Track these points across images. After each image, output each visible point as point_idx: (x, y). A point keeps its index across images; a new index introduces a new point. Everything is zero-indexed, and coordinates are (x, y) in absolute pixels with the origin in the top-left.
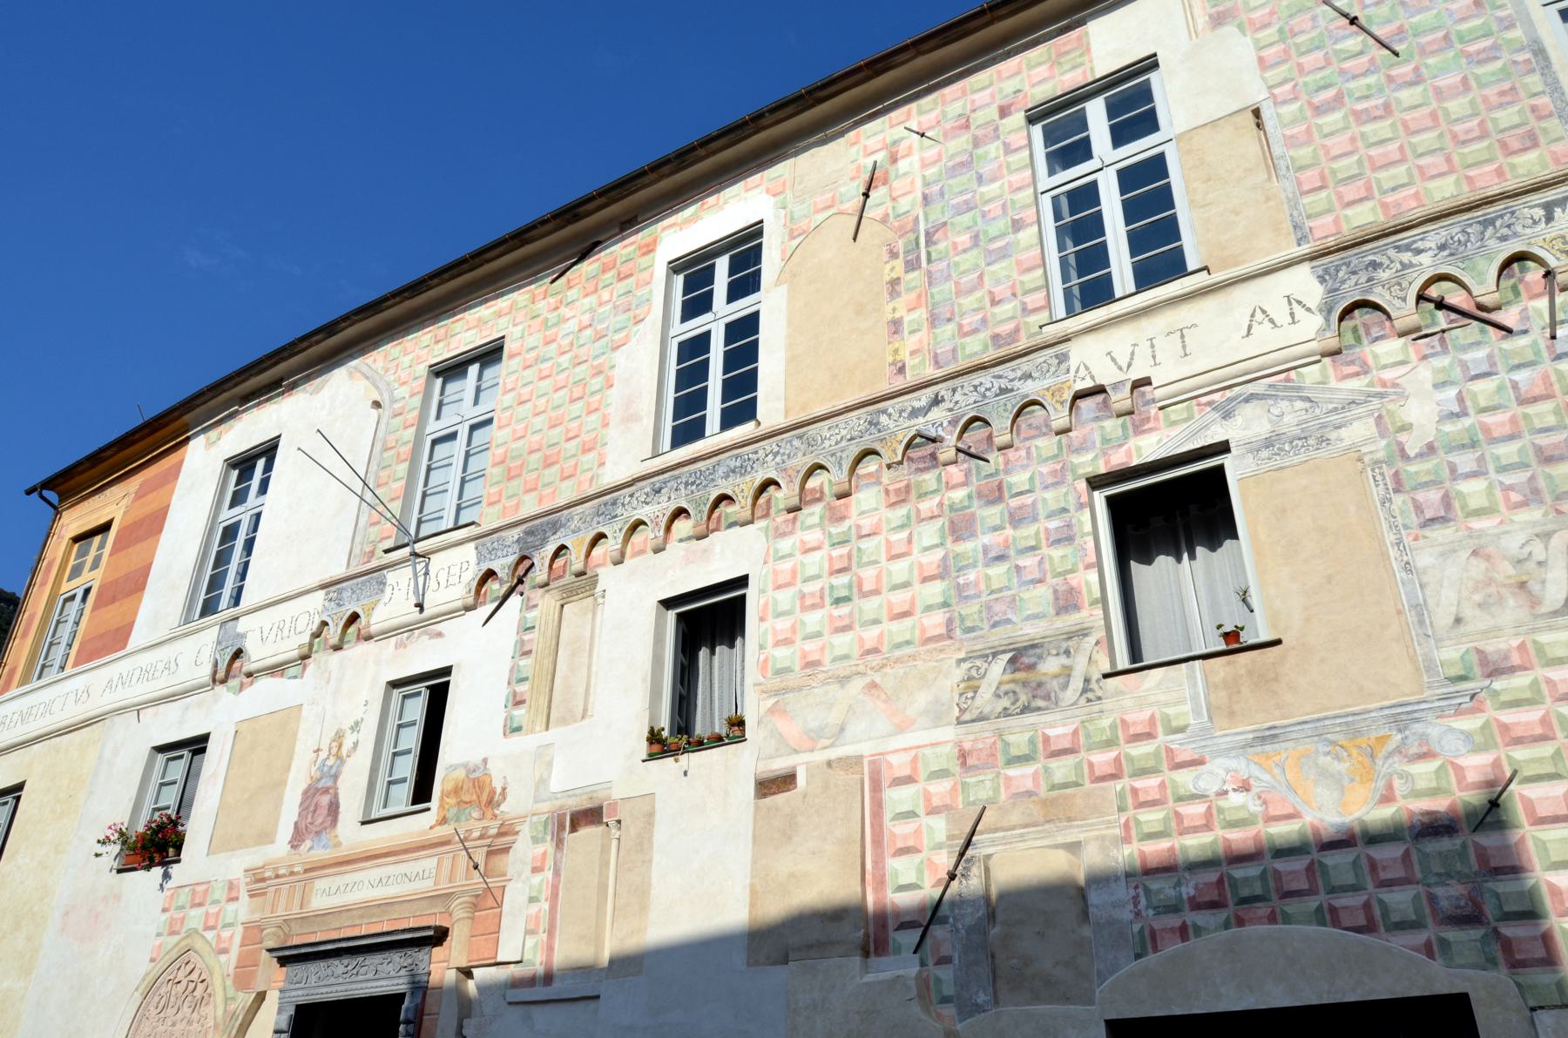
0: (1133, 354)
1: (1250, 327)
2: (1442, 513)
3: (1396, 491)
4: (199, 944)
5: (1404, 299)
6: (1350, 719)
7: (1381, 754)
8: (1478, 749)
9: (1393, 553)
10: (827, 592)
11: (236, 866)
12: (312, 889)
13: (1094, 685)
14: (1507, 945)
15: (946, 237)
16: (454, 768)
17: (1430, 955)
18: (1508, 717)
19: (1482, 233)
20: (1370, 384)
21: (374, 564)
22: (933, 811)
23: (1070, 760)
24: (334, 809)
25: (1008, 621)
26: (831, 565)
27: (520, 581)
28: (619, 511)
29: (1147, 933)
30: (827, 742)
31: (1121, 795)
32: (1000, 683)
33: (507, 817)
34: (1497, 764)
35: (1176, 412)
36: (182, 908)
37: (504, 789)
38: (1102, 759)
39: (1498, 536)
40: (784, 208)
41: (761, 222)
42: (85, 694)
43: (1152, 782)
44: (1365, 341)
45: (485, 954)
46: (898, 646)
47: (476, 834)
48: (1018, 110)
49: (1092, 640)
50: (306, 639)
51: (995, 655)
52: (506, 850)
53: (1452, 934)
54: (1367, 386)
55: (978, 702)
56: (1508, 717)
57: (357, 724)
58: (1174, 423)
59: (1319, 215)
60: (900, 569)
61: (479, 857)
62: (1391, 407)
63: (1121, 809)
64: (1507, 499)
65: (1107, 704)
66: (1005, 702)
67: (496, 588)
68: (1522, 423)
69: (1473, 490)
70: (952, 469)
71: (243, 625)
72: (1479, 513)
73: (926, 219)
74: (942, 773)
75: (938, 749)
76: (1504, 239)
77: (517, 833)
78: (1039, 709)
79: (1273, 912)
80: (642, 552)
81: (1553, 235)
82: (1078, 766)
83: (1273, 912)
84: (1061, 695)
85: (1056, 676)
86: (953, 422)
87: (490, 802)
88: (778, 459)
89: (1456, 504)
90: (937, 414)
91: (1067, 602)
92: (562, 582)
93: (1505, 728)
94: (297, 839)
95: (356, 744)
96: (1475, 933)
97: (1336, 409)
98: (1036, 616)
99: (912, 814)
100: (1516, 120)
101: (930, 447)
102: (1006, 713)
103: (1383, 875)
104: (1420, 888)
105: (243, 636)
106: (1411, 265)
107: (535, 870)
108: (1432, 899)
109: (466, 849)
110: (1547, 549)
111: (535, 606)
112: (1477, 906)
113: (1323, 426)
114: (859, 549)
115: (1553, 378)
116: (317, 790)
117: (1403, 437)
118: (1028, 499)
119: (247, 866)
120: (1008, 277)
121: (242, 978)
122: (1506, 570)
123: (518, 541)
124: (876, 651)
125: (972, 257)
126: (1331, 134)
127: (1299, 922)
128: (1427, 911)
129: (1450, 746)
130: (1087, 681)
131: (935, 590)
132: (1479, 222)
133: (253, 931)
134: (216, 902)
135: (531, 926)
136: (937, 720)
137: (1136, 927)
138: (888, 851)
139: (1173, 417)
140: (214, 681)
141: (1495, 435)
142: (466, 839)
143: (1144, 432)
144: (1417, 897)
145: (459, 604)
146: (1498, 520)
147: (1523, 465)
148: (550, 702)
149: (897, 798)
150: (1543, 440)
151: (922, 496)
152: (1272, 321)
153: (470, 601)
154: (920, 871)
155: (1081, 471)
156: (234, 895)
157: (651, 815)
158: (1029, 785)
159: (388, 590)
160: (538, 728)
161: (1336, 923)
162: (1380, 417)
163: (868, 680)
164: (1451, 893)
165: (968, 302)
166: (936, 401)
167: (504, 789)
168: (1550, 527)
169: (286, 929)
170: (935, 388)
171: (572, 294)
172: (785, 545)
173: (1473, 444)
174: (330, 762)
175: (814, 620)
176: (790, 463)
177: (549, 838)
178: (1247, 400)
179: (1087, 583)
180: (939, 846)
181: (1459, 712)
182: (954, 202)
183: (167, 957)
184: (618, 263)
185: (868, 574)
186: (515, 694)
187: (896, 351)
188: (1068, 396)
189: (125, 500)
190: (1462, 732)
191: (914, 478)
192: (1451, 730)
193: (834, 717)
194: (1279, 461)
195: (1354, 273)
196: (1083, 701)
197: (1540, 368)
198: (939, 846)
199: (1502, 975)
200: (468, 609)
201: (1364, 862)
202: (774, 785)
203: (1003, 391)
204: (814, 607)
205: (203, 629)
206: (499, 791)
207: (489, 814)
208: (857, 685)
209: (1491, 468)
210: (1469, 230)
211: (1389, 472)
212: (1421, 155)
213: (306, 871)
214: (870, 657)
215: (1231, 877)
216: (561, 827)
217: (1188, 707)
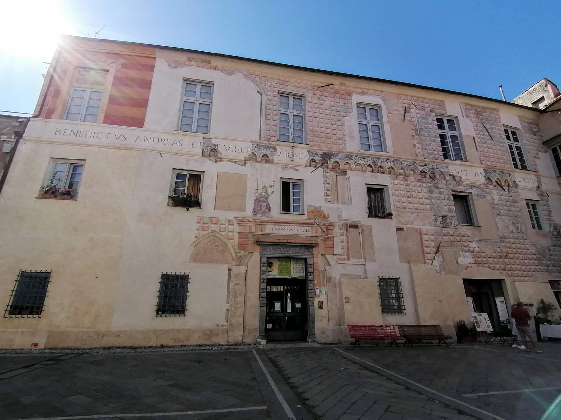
8: (504, 248)
22: (431, 241)
25: (441, 211)
32: (441, 222)
37: (328, 215)
38: (458, 238)
43: (466, 243)
46: (422, 209)
49: (455, 218)
51: (439, 216)
52: (333, 229)
60: (420, 195)
61: (325, 229)
63: (461, 247)
87: (324, 217)
90: (425, 167)
91: (450, 211)
92: (335, 170)
93: (507, 246)
94: (255, 212)
95: (273, 192)
96: (505, 272)
99: (428, 241)
101: (424, 174)
102: (442, 227)
105: (215, 145)
107: (341, 235)
112: (505, 268)
113: (484, 195)
117: (494, 201)
123: (321, 155)
124: (417, 209)
125: (428, 139)
131: (427, 201)
135: (342, 248)
136: (431, 224)
137: (465, 265)
149: (425, 237)
151: (423, 182)
153: (309, 165)
157: (371, 230)
158: (447, 240)
167: (328, 215)
169: (257, 237)
170: (426, 162)
172: (396, 182)
174: (264, 194)
175: (404, 199)
177: (344, 229)
180: (433, 247)
183: (203, 237)
185: (414, 194)
187: (415, 151)
193: (411, 219)
198: (433, 247)
199: (508, 277)
203: (437, 168)
206: (327, 215)
208: (414, 215)
213: (261, 222)
216: (347, 227)
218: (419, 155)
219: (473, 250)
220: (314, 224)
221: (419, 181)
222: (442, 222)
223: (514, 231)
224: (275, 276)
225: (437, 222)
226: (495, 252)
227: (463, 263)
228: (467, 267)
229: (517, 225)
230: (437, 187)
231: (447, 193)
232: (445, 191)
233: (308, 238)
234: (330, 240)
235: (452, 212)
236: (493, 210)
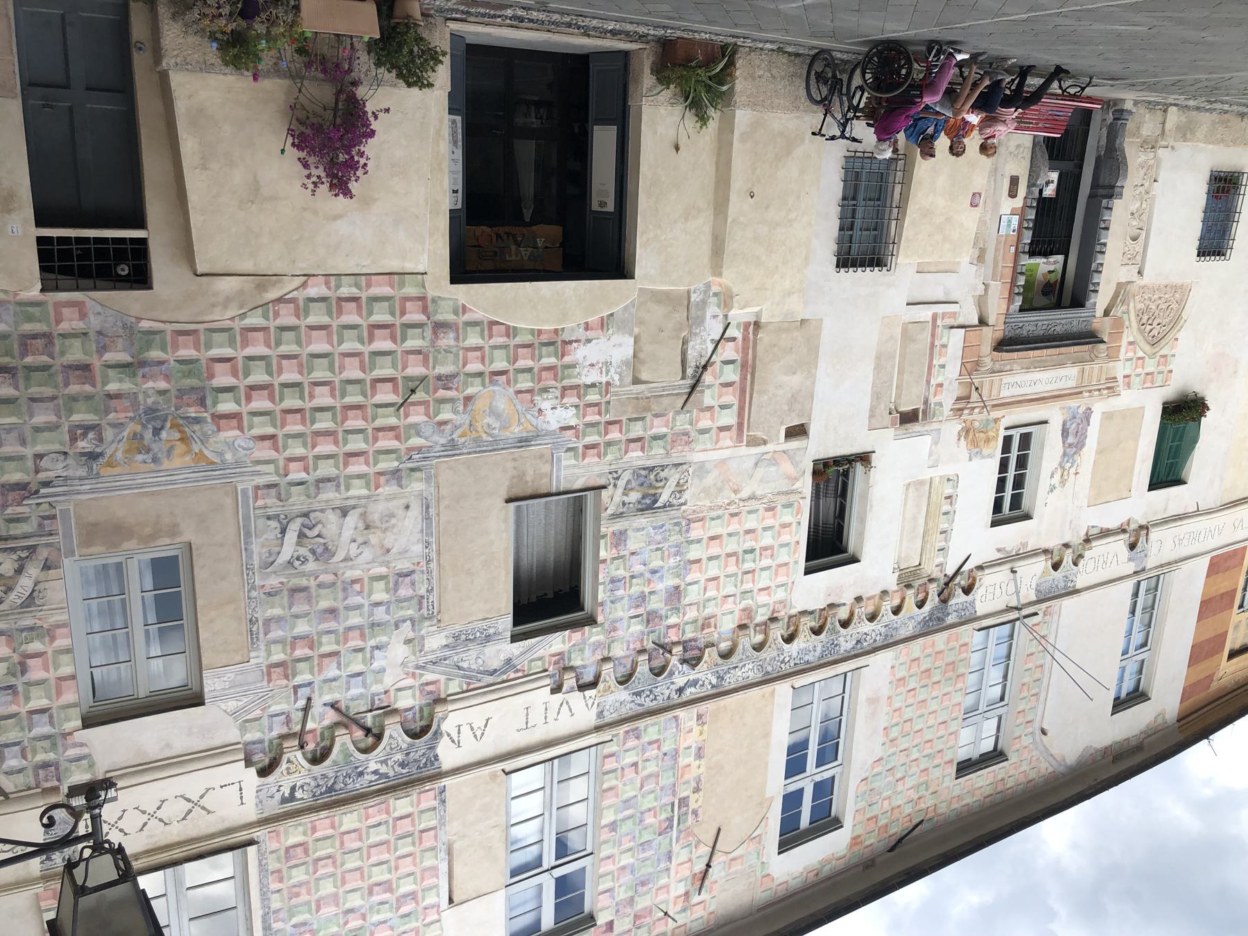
0: (558, 713)
1: (486, 726)
2: (401, 579)
3: (422, 597)
4: (1147, 348)
5: (391, 737)
6: (478, 449)
7: (466, 426)
8: (414, 426)
9: (434, 555)
10: (758, 558)
11: (1126, 399)
12: (1077, 380)
13: (612, 481)
14: (425, 310)
15: (660, 823)
16: (990, 456)
17: (464, 307)
18: (394, 444)
19: (335, 782)
20: (422, 675)
21: (1044, 605)
22: (710, 408)
23: (632, 435)
24: (1065, 433)
26: (754, 576)
27: (947, 584)
28: (883, 630)
29: (605, 328)
30: (765, 456)
31: (607, 411)
32: (663, 487)
33: (957, 421)
34: (407, 415)
35: (538, 666)
36: (1159, 373)
38: (614, 435)
39: (373, 561)
40: (763, 863)
41: (779, 853)
42: (1236, 525)
43: (589, 419)
44: (417, 708)
45: (972, 334)
46: (719, 517)
47: (977, 410)
48: (601, 926)
49: (609, 512)
50: (1087, 554)
51: (665, 506)
52: (958, 399)
53: (450, 317)
54: (423, 675)
55: (677, 476)
56: (394, 444)
57: (1052, 491)
58: (540, 659)
59: (429, 810)
60: (713, 569)
61: (975, 396)
62: (413, 658)
63: (608, 403)
64: (362, 587)
65: (607, 469)
66: (662, 475)
67: (961, 580)
69: (380, 595)
70: (675, 639)
71: (1131, 568)
72: (380, 578)
73: (671, 840)
74: (703, 432)
75: (704, 447)
76: (324, 776)
77: (952, 410)
78: (644, 469)
79: (539, 336)
80: (869, 599)
81: (294, 776)
82: (628, 431)
83: (539, 336)
84: (631, 477)
85: (632, 489)
86: (671, 674)
87: (968, 432)
88: (782, 657)
89: (391, 585)
90: (680, 681)
91: (620, 538)
93: (398, 438)
95: (1052, 476)
96: (440, 317)
97: (445, 660)
98: (638, 530)
99: (722, 407)
100: (294, 872)
101: (688, 655)
102: (663, 468)
103: (478, 354)
104: (461, 345)
105: (1130, 560)
106: (382, 762)
107: (941, 385)
108: (457, 339)
109: (983, 401)
111: (937, 566)
112: (435, 333)
113: (454, 648)
114: (736, 587)
115: (316, 669)
116: (1076, 447)
117: (411, 635)
118: (633, 612)
119: (1118, 397)
120: (625, 785)
121: (1119, 325)
122: (374, 539)
123: (948, 614)
124: (733, 515)
126: (409, 875)
127: (526, 329)
128: (461, 331)
129: (428, 431)
130: (615, 485)
131: (694, 553)
132: (335, 791)
133: (1113, 356)
134: (1138, 375)
135: (944, 350)
136: (702, 468)
137: (610, 331)
138: (737, 385)
139: (539, 663)
140: (1147, 528)
142: (983, 408)
143: (558, 654)
144: (464, 340)
145: (987, 571)
147: (347, 608)
148: (929, 497)
149: (729, 418)
150: (332, 625)
152: (472, 729)
154: (721, 371)
155: (599, 629)
156: (1127, 379)
158: (657, 421)
159: (1034, 586)
160: (937, 479)
161: (508, 327)
162: (421, 651)
163: (739, 496)
164: (447, 340)
165: (652, 768)
166: (680, 691)
168: (342, 565)
169: (1092, 355)
170: (680, 701)
171: (908, 810)
172: (780, 594)
173: (373, 625)
174: (1069, 465)
175: (767, 539)
176: (775, 653)
178: (495, 671)
179: (606, 550)
180: (709, 387)
181: (419, 449)
182: (652, 852)
184: (876, 832)
185: (732, 569)
186: (951, 504)
187: (701, 733)
188: (601, 686)
189: (1220, 675)
190: (421, 437)
191: (698, 635)
192: (426, 439)
193: (760, 472)
194: (484, 624)
195: (415, 761)
196: (620, 472)
197: (322, 677)
198: (709, 387)
199: (431, 293)
200: (980, 568)
201: (487, 362)
202: (797, 432)
203: (638, 694)
204: (766, 549)
205: (1156, 567)
206: (962, 438)
207: (968, 423)
208: (745, 494)
209: (366, 608)
210: (342, 785)
211: (424, 611)
212: (358, 850)
213: (1081, 393)
214: (737, 511)
215: (557, 358)
216: (925, 412)
217: (564, 463)
218: (693, 723)
219: (563, 396)
220: (994, 406)
221: (706, 623)
222: (661, 484)
223: (332, 517)
224: (1045, 260)
225: (678, 484)
226: (468, 399)
227: (616, 338)
228: (603, 324)
229: (303, 551)
230: (651, 618)
231: (618, 605)
232: (620, 614)
233: (1008, 367)
234: (968, 366)
235: (614, 534)
236: (430, 591)
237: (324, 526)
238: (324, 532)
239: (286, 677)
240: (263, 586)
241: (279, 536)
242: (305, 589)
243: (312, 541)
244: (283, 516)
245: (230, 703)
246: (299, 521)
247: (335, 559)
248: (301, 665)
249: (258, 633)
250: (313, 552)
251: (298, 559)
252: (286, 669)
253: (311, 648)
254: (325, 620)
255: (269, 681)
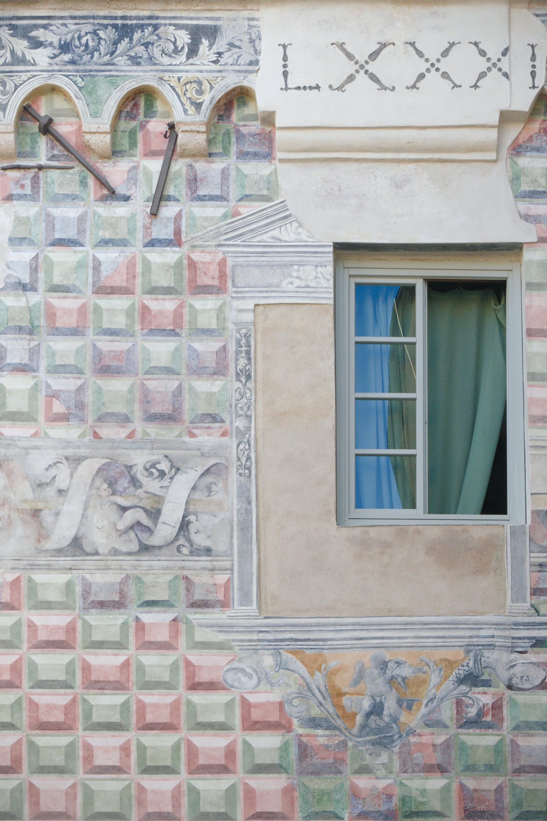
39: (27, 450)
64: (49, 406)
68: (91, 317)
110: (72, 476)
115: (139, 269)
141: (58, 325)
146: (33, 431)
147: (78, 371)
168: (82, 452)
173: (31, 331)
197: (129, 251)
209: (43, 364)
237: (115, 524)
238: (113, 514)
239: (192, 265)
240: (224, 434)
241: (192, 518)
242: (152, 418)
243: (135, 502)
244: (185, 551)
245: (293, 237)
246: (156, 540)
247: (97, 463)
248: (165, 281)
249: (237, 353)
250: (135, 482)
251: (162, 474)
252: (192, 280)
253: (145, 310)
254: (117, 356)
255: (222, 264)
